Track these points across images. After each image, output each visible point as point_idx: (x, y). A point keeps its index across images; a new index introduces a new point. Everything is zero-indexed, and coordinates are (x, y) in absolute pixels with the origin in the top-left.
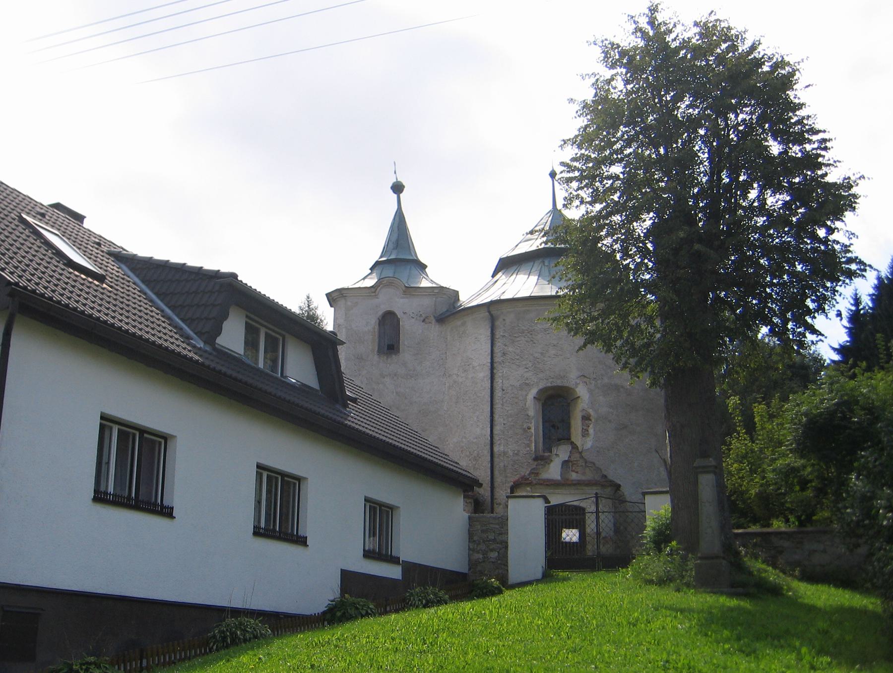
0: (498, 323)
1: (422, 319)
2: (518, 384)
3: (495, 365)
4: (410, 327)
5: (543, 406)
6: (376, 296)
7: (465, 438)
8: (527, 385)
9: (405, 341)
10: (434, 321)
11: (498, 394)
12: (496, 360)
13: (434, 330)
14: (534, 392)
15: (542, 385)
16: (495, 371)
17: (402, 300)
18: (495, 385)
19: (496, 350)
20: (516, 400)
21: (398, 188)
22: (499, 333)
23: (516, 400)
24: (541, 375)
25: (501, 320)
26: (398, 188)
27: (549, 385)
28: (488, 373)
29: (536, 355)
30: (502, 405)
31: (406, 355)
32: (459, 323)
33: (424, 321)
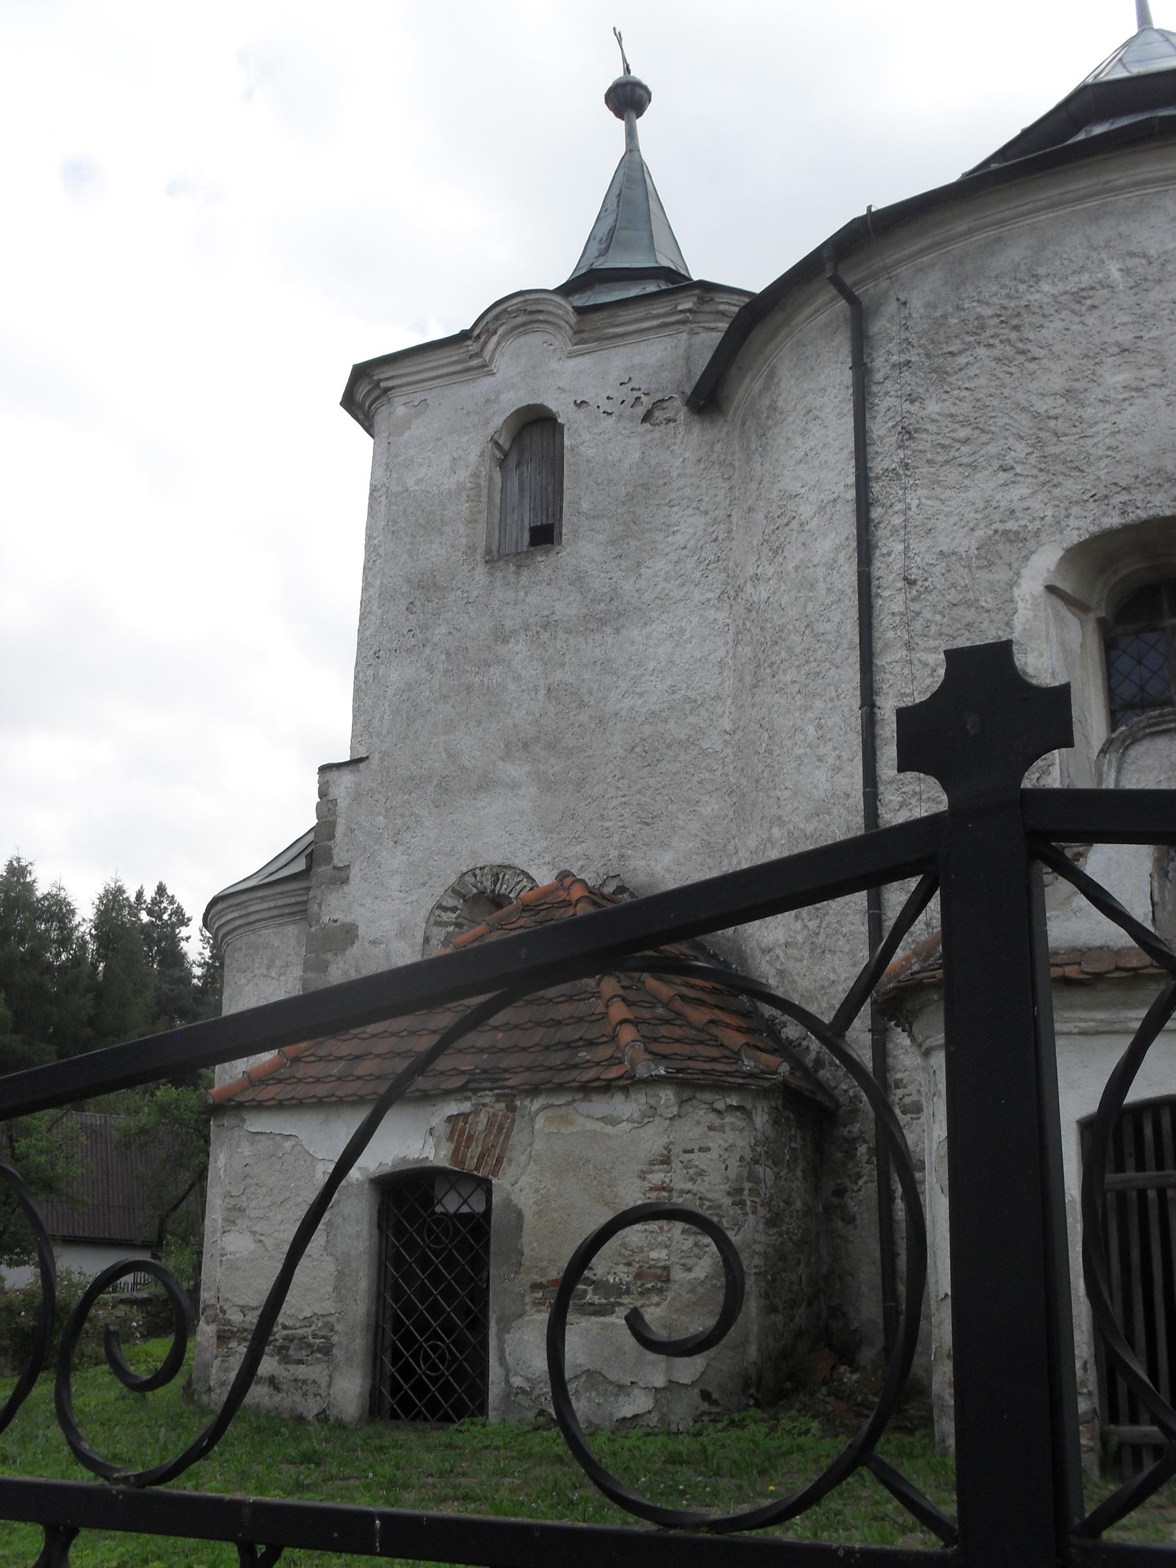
0: (880, 325)
1: (640, 411)
2: (967, 544)
3: (876, 488)
4: (598, 448)
5: (1109, 645)
6: (485, 369)
7: (780, 821)
8: (1008, 541)
9: (578, 497)
10: (683, 414)
11: (891, 603)
12: (878, 466)
13: (685, 444)
14: (1045, 562)
15: (1080, 527)
16: (876, 513)
17: (571, 364)
18: (879, 568)
19: (879, 428)
20: (971, 615)
21: (627, 99)
22: (880, 364)
23: (971, 615)
24: (1071, 487)
25: (892, 307)
26: (627, 99)
27: (1114, 520)
28: (849, 528)
29: (1042, 406)
30: (909, 647)
31: (582, 547)
32: (757, 386)
33: (647, 417)
